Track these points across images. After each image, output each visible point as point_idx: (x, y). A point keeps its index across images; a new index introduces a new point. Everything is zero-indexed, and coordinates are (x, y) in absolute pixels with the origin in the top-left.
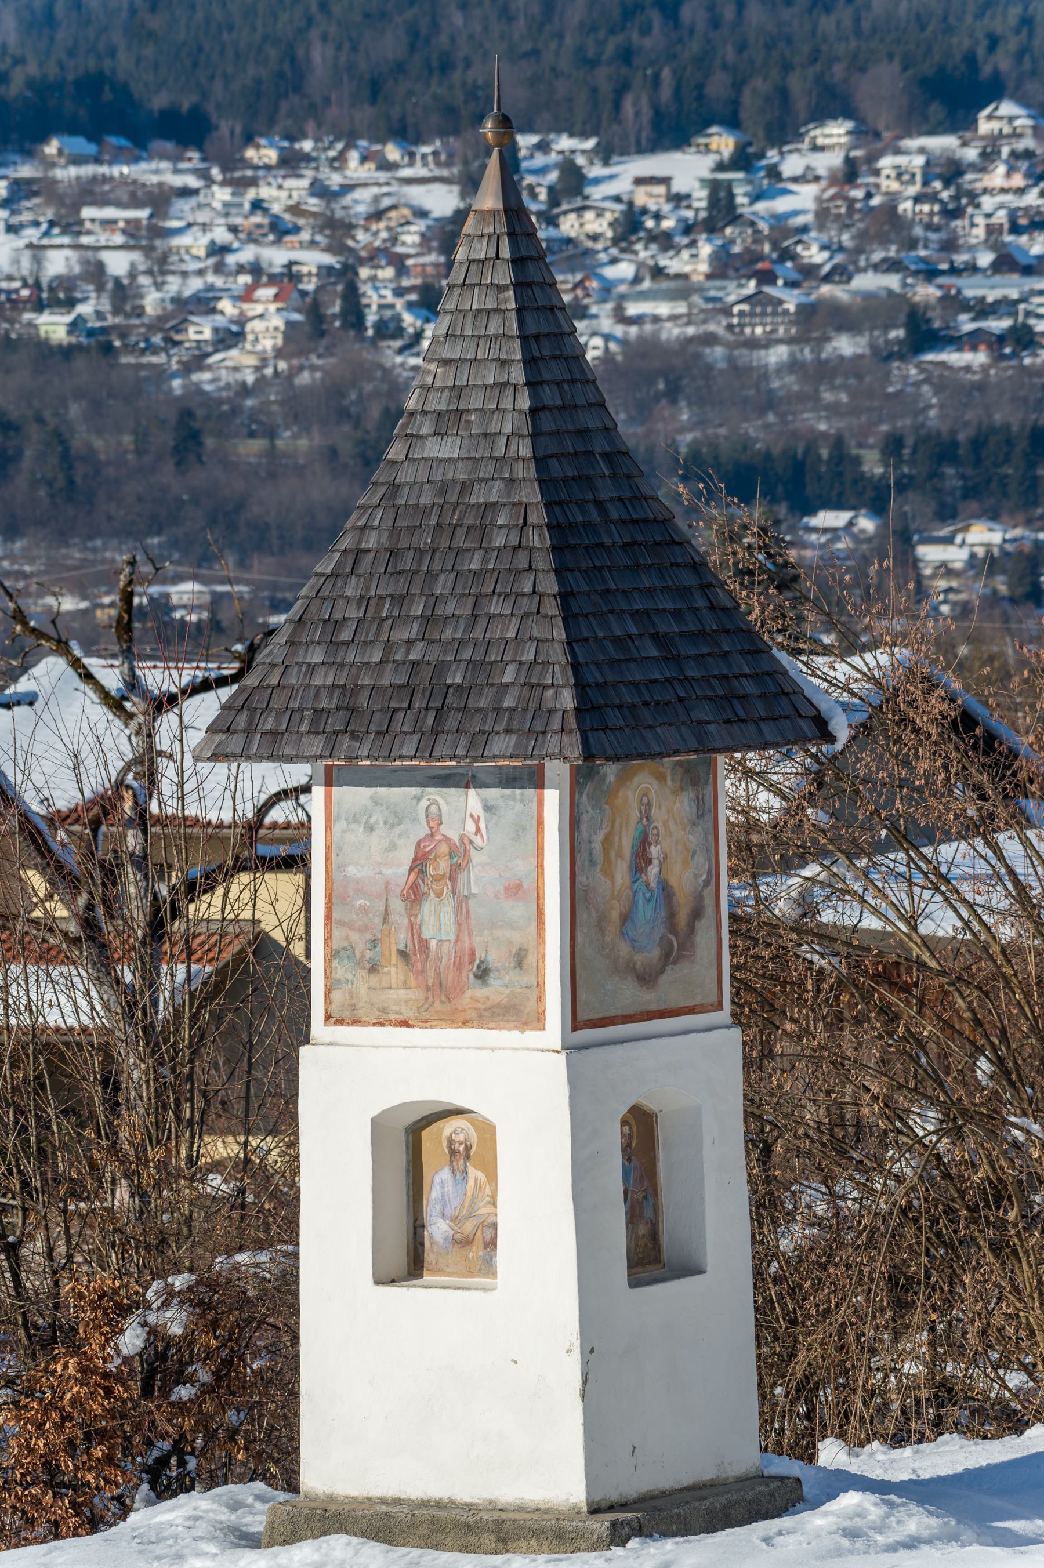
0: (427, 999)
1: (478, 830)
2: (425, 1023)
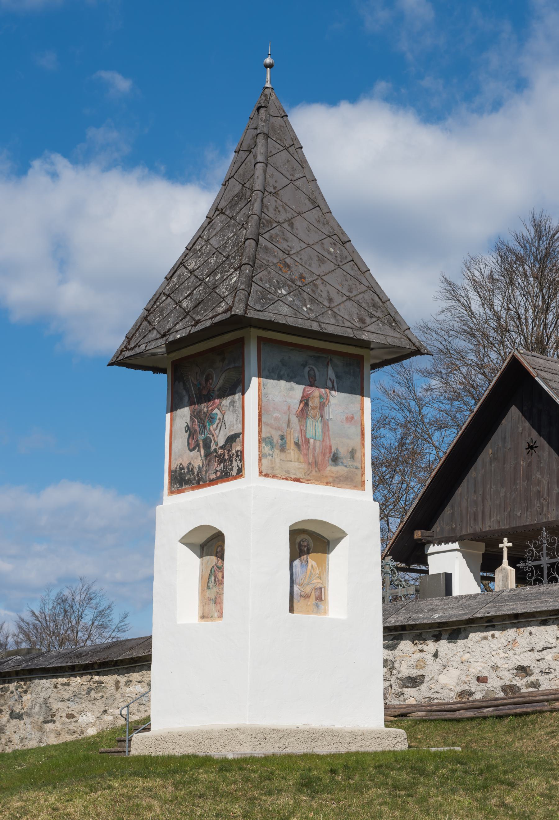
0: (308, 469)
2: (308, 481)
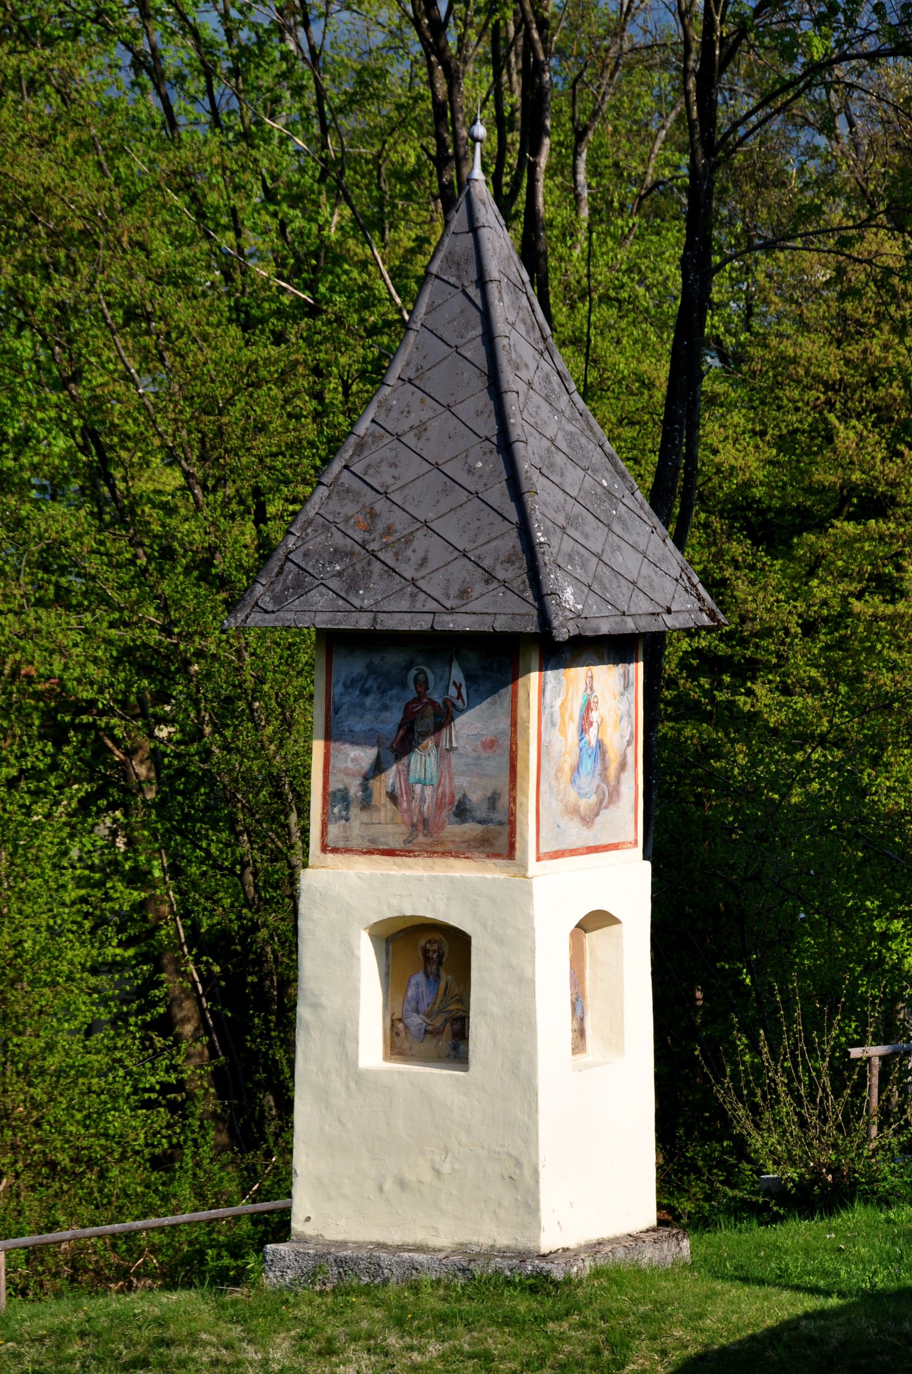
1: (460, 695)
2: (407, 853)
